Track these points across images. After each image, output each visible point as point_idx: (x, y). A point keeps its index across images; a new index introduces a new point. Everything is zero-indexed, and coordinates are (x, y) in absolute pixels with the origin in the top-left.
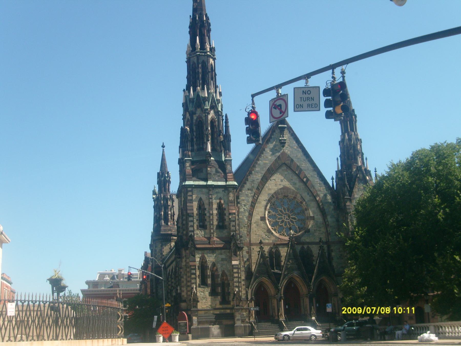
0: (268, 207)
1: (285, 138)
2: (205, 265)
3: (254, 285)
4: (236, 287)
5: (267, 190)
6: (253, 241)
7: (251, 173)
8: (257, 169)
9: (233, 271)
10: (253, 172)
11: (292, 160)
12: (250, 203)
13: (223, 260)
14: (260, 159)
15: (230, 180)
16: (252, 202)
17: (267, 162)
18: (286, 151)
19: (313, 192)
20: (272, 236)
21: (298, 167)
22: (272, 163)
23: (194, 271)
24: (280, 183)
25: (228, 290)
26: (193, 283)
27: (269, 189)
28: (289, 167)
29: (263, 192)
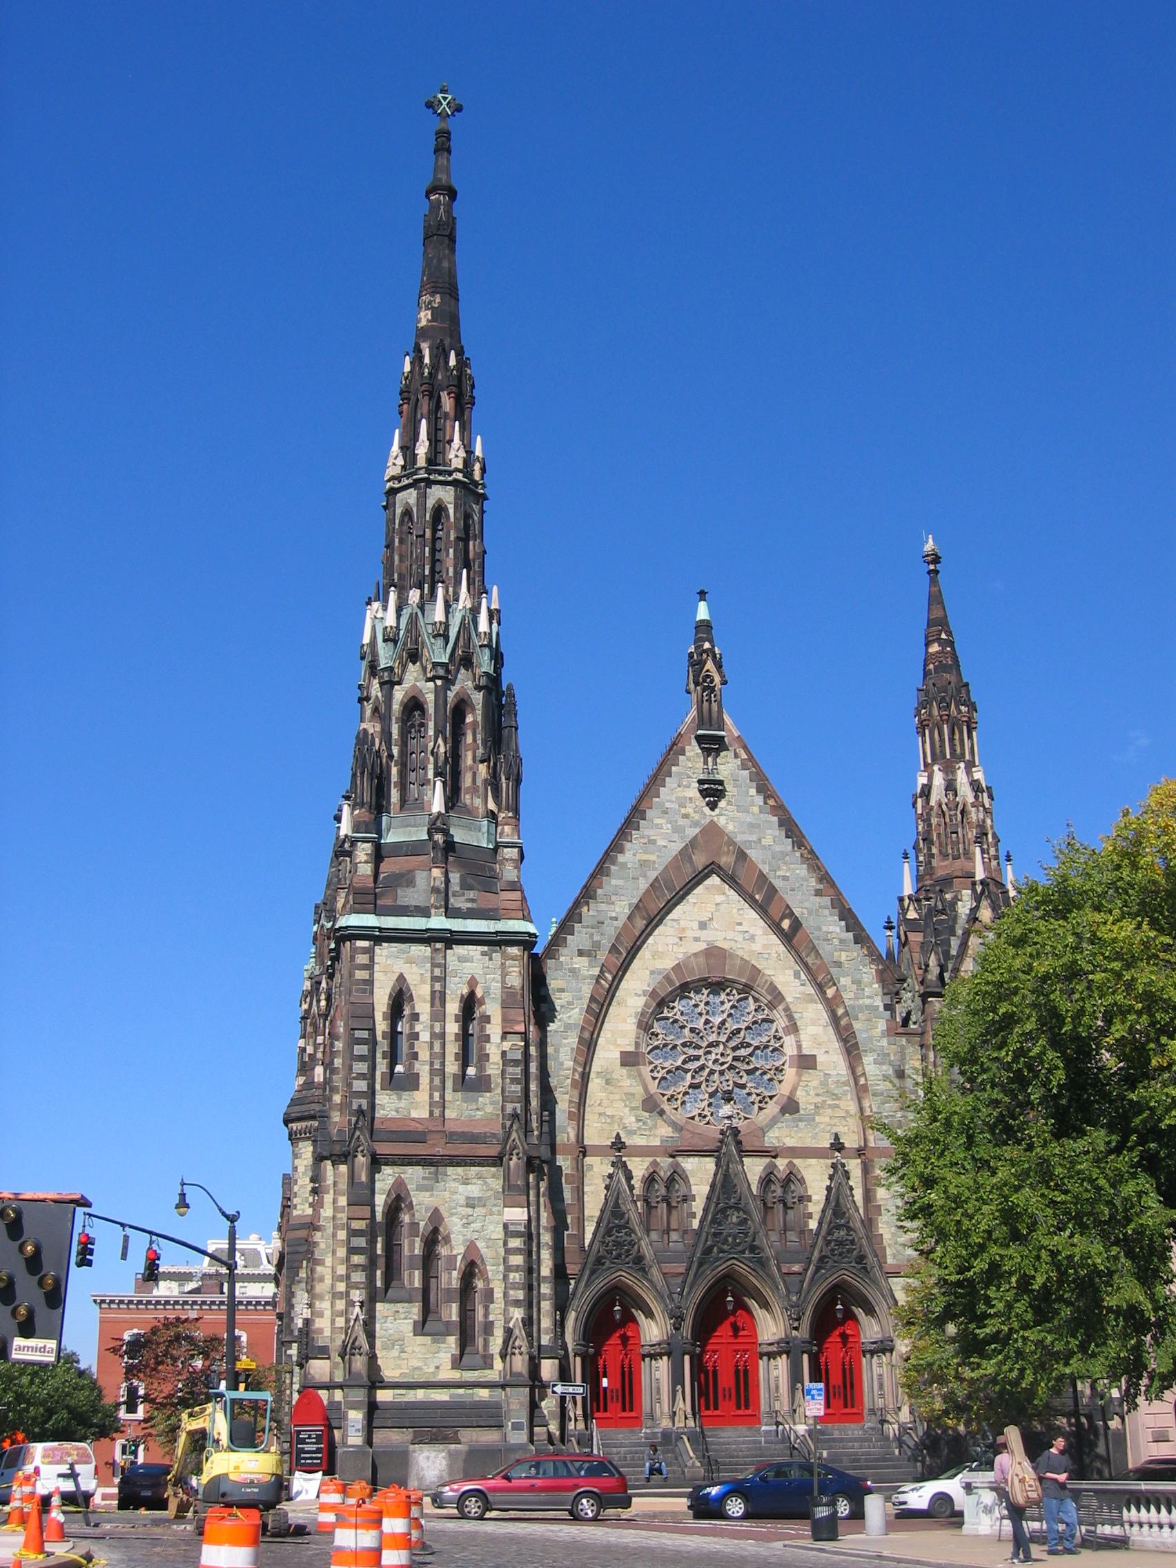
10: (599, 891)
11: (742, 856)
13: (471, 1203)
15: (513, 914)
17: (653, 857)
20: (660, 1121)
21: (762, 877)
22: (666, 863)
24: (698, 934)
25: (486, 1315)
28: (731, 880)
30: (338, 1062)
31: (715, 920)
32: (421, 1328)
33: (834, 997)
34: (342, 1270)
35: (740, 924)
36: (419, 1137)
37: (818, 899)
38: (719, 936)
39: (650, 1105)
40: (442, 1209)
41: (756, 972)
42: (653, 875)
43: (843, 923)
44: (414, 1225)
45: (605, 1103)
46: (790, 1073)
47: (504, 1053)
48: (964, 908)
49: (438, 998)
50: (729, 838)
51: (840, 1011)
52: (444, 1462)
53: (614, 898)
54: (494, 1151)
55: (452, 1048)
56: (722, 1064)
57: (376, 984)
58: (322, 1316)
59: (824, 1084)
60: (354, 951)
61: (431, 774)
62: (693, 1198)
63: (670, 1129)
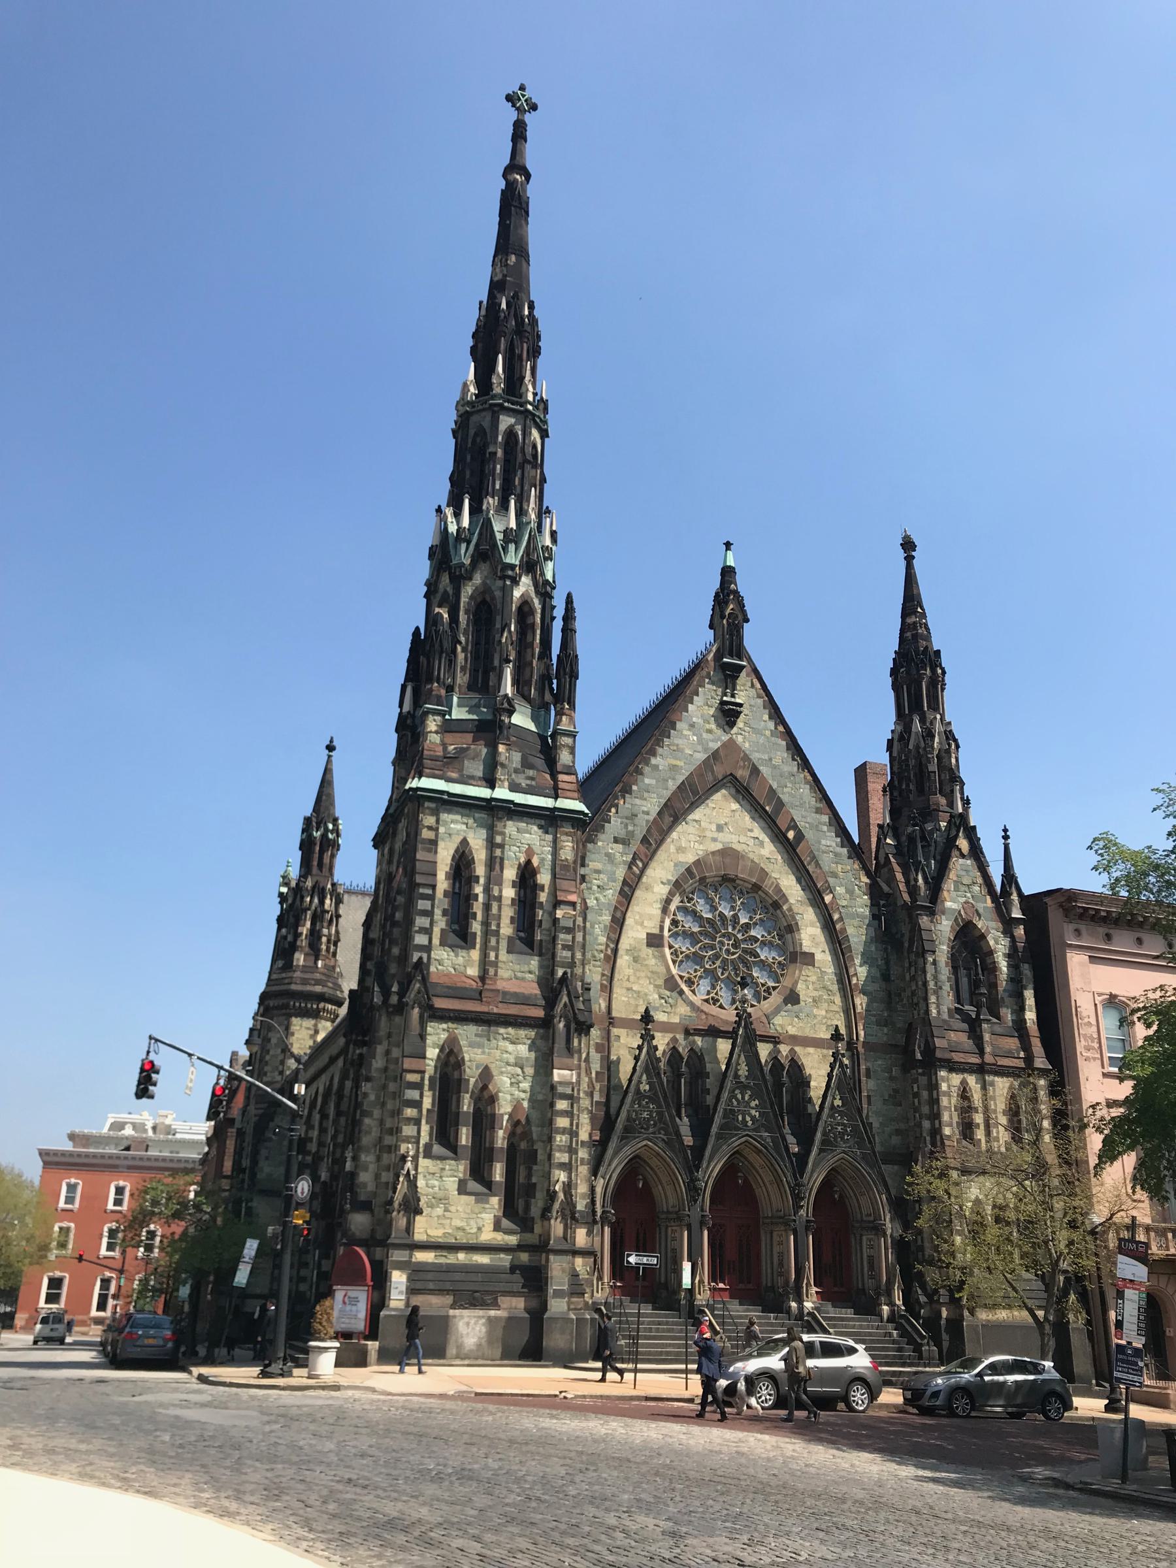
0: (673, 907)
1: (738, 701)
2: (456, 1075)
3: (615, 1166)
4: (562, 1166)
5: (672, 849)
7: (626, 790)
8: (647, 781)
9: (552, 1105)
10: (634, 788)
11: (755, 771)
14: (660, 750)
16: (625, 882)
17: (678, 763)
18: (740, 739)
19: (814, 876)
20: (680, 999)
23: (413, 1094)
24: (715, 835)
25: (529, 1176)
26: (407, 1140)
27: (680, 850)
29: (661, 855)
33: (832, 903)
35: (751, 831)
37: (818, 816)
39: (671, 983)
40: (492, 1067)
41: (764, 874)
42: (680, 779)
43: (839, 840)
45: (632, 979)
50: (745, 755)
51: (836, 917)
52: (484, 1329)
53: (646, 795)
54: (540, 1013)
56: (734, 954)
58: (366, 1170)
63: (688, 1009)
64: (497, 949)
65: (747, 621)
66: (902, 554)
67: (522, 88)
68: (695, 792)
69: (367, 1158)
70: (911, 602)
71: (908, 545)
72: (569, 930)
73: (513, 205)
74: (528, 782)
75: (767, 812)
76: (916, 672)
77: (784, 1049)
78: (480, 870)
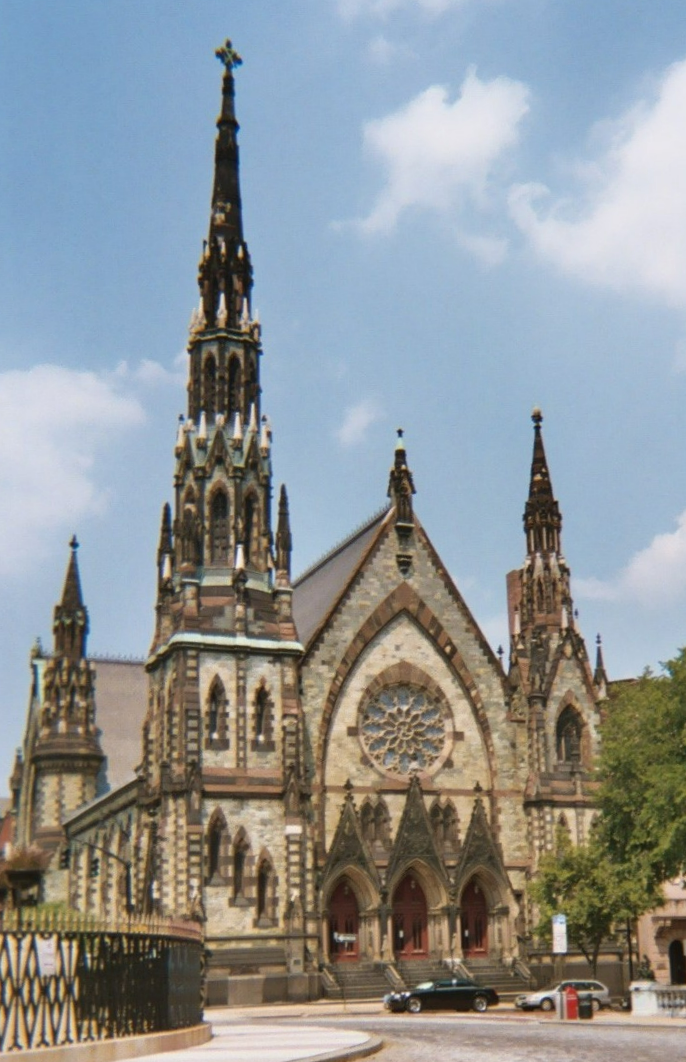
6: (329, 782)
10: (335, 624)
11: (422, 605)
12: (326, 694)
13: (264, 823)
16: (331, 693)
17: (368, 603)
19: (464, 678)
21: (434, 620)
23: (195, 848)
25: (274, 892)
28: (415, 620)
30: (175, 731)
31: (403, 646)
32: (232, 902)
34: (183, 866)
35: (419, 648)
36: (231, 781)
37: (467, 634)
38: (407, 655)
39: (365, 760)
40: (245, 826)
41: (428, 679)
42: (368, 614)
44: (228, 837)
46: (448, 743)
47: (284, 728)
48: (554, 644)
49: (241, 691)
51: (479, 706)
54: (278, 790)
55: (251, 723)
56: (408, 736)
57: (201, 680)
59: (469, 749)
60: (186, 657)
61: (232, 541)
62: (390, 819)
64: (244, 749)
65: (414, 492)
66: (533, 424)
67: (229, 45)
68: (379, 624)
69: (169, 889)
70: (539, 463)
71: (537, 418)
72: (292, 733)
73: (227, 156)
74: (260, 630)
75: (433, 633)
76: (542, 515)
77: (443, 799)
78: (231, 696)
